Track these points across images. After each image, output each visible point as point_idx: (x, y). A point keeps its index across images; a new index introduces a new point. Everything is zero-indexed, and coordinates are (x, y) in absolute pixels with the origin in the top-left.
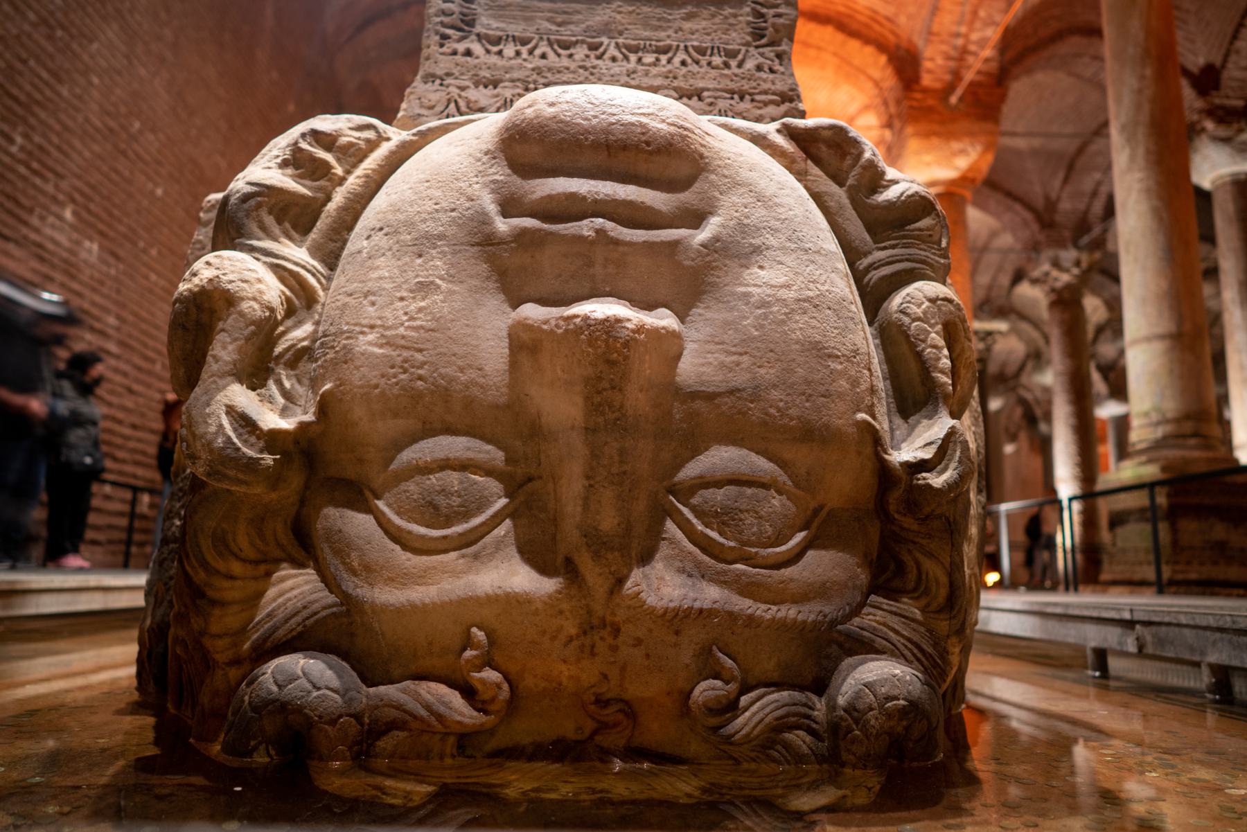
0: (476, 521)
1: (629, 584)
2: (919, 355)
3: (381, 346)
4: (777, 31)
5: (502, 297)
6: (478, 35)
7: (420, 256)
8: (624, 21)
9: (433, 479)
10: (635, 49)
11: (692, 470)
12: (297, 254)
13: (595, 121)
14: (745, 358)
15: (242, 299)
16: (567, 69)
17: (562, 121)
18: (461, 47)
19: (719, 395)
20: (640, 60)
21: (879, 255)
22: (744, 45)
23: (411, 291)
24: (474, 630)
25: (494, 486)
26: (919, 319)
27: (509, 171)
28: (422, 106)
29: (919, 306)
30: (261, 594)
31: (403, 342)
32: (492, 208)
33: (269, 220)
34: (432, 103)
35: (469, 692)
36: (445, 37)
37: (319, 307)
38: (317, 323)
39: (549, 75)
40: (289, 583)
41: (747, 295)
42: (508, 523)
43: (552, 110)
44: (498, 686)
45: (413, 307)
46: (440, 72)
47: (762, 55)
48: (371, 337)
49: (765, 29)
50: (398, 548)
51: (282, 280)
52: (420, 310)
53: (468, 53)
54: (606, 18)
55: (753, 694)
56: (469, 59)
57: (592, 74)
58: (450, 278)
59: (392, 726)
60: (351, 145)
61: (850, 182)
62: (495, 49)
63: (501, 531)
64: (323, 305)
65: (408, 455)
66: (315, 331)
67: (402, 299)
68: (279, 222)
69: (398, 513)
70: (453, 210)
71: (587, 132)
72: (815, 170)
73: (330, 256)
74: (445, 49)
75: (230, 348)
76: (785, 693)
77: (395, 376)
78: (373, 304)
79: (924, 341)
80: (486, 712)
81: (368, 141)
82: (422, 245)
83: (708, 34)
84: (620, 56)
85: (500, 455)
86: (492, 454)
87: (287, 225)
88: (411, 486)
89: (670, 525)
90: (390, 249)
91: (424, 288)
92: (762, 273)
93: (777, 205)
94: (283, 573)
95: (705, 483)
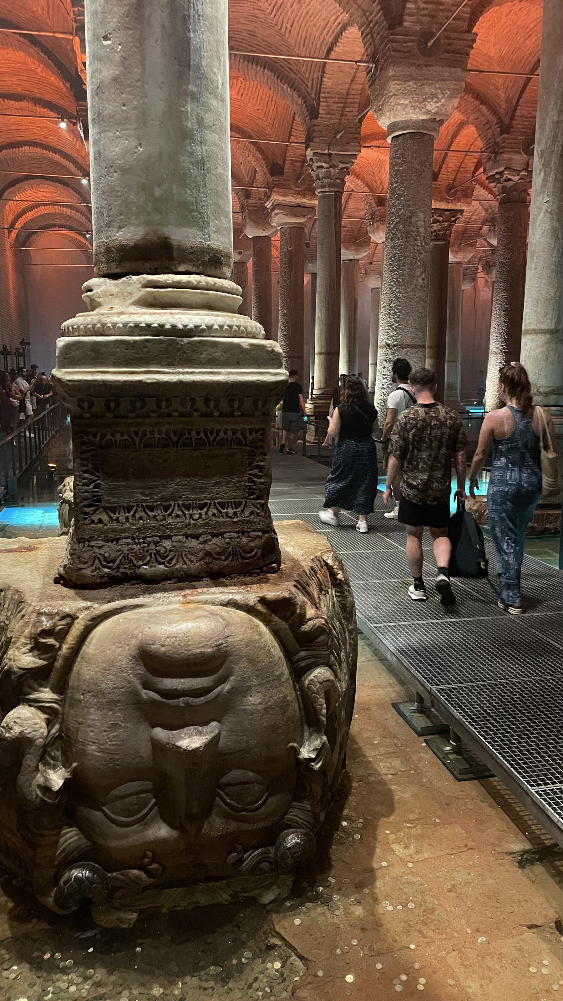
0: (145, 811)
1: (203, 830)
2: (314, 708)
3: (99, 752)
4: (261, 492)
5: (147, 723)
6: (104, 508)
7: (111, 711)
8: (181, 490)
9: (126, 800)
10: (188, 508)
11: (225, 779)
12: (46, 694)
13: (182, 655)
14: (245, 737)
15: (36, 739)
16: (154, 527)
17: (168, 656)
18: (95, 518)
19: (233, 753)
20: (191, 515)
21: (302, 654)
22: (244, 498)
23: (109, 728)
24: (148, 852)
25: (150, 795)
26: (315, 693)
27: (145, 669)
28: (81, 562)
29: (315, 686)
30: (58, 841)
31: (109, 751)
32: (140, 687)
33: (32, 682)
34: (85, 561)
35: (147, 871)
36: (86, 514)
37: (60, 716)
38: (61, 723)
39: (144, 531)
40: (68, 835)
41: (246, 710)
42: (156, 808)
43: (163, 649)
44: (158, 869)
45: (111, 735)
46: (87, 537)
47: (253, 505)
48: (94, 747)
49: (255, 490)
50: (114, 826)
51: (44, 713)
52: (114, 737)
53: (100, 521)
54: (172, 490)
55: (248, 854)
56: (101, 525)
57: (167, 528)
58: (125, 721)
59: (119, 888)
60: (61, 629)
61: (290, 622)
62: (114, 516)
63: (153, 812)
64: (63, 714)
65: (117, 792)
66: (61, 727)
67: (105, 731)
68: (36, 680)
69: (113, 813)
70: (122, 688)
71: (179, 660)
72: (276, 619)
73: (61, 688)
74: (87, 522)
75: (34, 760)
76: (260, 850)
77: (107, 765)
78: (92, 731)
79: (316, 702)
80: (154, 878)
81: (67, 624)
82: (111, 705)
83: (226, 494)
84: (180, 513)
85: (151, 783)
86: (148, 784)
87: (39, 680)
88: (118, 803)
89: (217, 798)
90: (96, 705)
91: (114, 726)
92: (251, 699)
93: (259, 662)
94: (65, 831)
95: (230, 784)
